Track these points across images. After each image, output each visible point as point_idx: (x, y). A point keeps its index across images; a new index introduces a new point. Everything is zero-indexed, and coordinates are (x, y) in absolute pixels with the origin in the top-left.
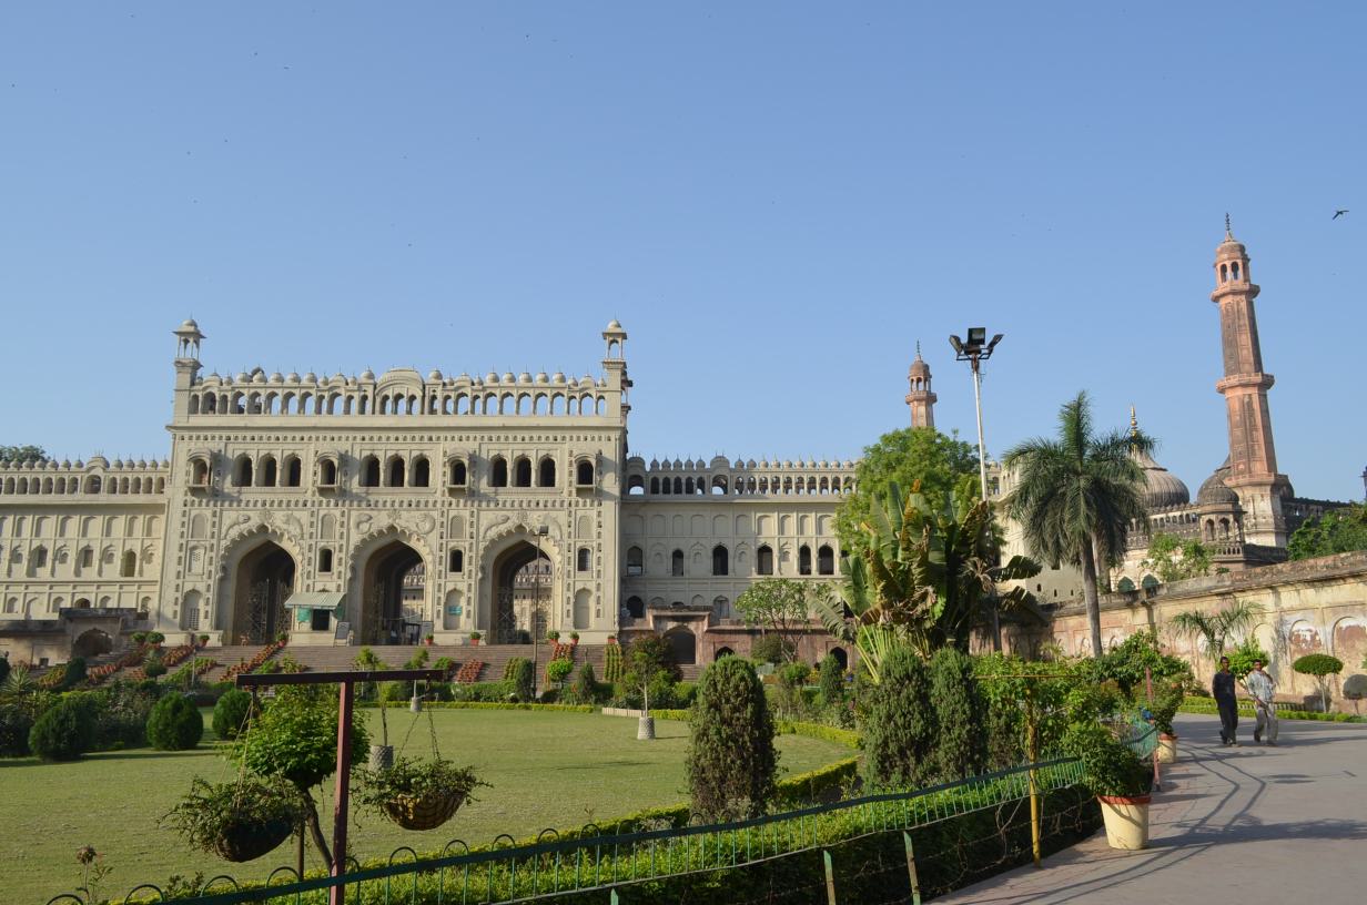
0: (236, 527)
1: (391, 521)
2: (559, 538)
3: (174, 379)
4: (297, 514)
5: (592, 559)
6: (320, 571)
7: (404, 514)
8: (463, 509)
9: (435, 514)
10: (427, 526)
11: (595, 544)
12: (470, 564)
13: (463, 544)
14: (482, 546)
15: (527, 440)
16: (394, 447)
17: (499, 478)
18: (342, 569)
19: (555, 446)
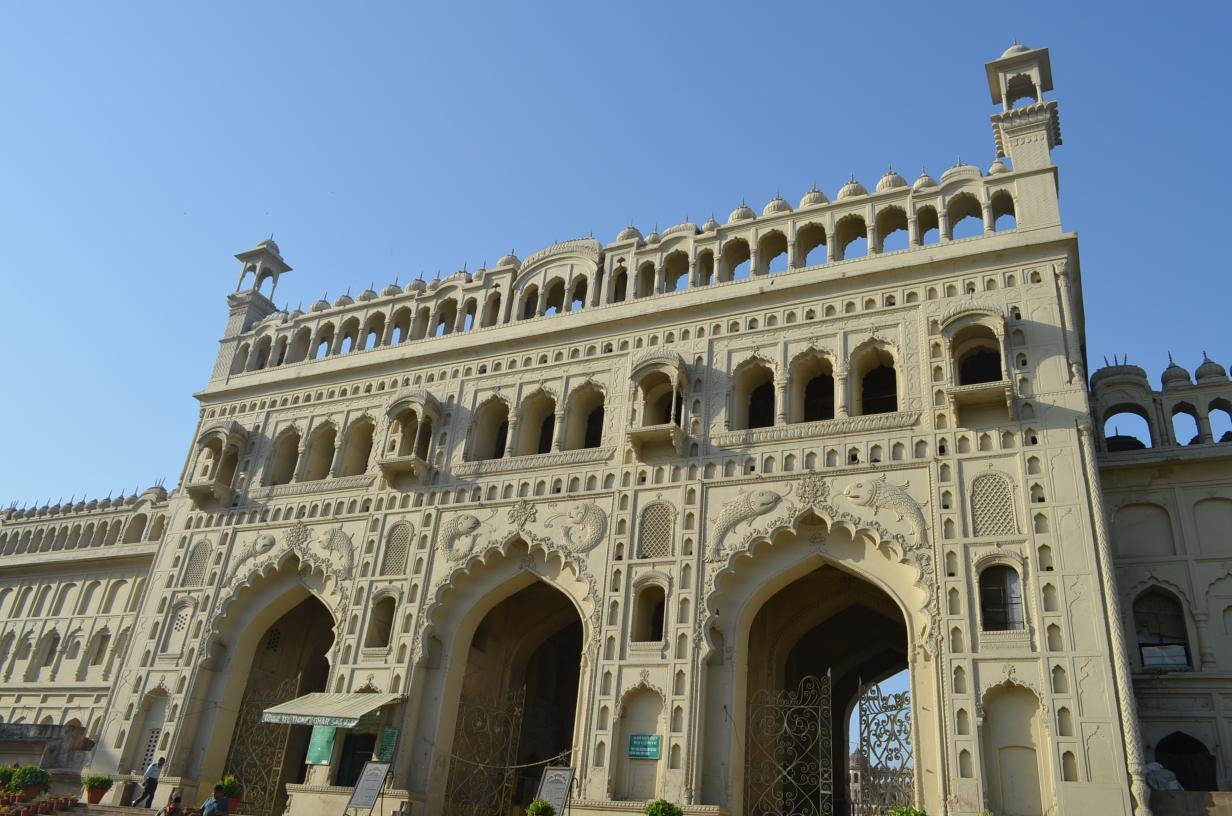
0: (251, 562)
1: (515, 527)
2: (916, 539)
3: (223, 322)
4: (349, 528)
5: (1026, 594)
6: (368, 645)
7: (543, 511)
8: (670, 490)
9: (606, 504)
10: (588, 533)
11: (1028, 551)
12: (682, 619)
13: (664, 570)
14: (711, 571)
15: (819, 316)
16: (536, 376)
17: (757, 409)
18: (407, 639)
19: (890, 319)
